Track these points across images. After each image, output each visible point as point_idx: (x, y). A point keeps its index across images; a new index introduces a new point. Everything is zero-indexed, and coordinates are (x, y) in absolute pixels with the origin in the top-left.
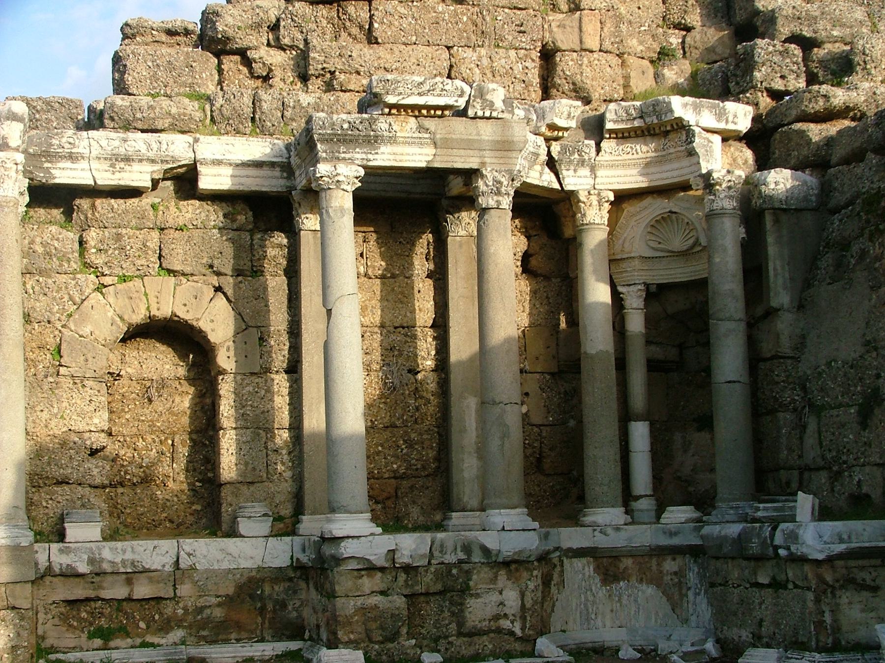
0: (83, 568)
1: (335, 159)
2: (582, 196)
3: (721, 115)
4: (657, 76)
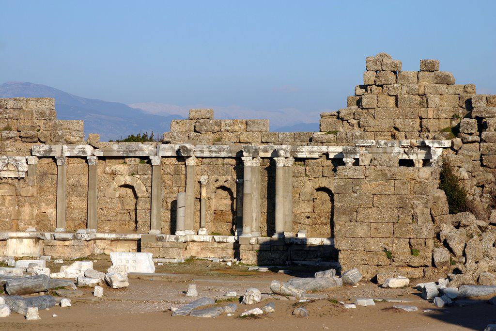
0: (300, 243)
1: (347, 157)
2: (414, 161)
3: (440, 143)
4: (451, 123)
